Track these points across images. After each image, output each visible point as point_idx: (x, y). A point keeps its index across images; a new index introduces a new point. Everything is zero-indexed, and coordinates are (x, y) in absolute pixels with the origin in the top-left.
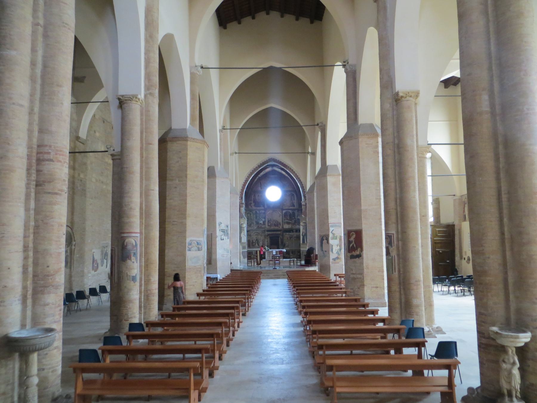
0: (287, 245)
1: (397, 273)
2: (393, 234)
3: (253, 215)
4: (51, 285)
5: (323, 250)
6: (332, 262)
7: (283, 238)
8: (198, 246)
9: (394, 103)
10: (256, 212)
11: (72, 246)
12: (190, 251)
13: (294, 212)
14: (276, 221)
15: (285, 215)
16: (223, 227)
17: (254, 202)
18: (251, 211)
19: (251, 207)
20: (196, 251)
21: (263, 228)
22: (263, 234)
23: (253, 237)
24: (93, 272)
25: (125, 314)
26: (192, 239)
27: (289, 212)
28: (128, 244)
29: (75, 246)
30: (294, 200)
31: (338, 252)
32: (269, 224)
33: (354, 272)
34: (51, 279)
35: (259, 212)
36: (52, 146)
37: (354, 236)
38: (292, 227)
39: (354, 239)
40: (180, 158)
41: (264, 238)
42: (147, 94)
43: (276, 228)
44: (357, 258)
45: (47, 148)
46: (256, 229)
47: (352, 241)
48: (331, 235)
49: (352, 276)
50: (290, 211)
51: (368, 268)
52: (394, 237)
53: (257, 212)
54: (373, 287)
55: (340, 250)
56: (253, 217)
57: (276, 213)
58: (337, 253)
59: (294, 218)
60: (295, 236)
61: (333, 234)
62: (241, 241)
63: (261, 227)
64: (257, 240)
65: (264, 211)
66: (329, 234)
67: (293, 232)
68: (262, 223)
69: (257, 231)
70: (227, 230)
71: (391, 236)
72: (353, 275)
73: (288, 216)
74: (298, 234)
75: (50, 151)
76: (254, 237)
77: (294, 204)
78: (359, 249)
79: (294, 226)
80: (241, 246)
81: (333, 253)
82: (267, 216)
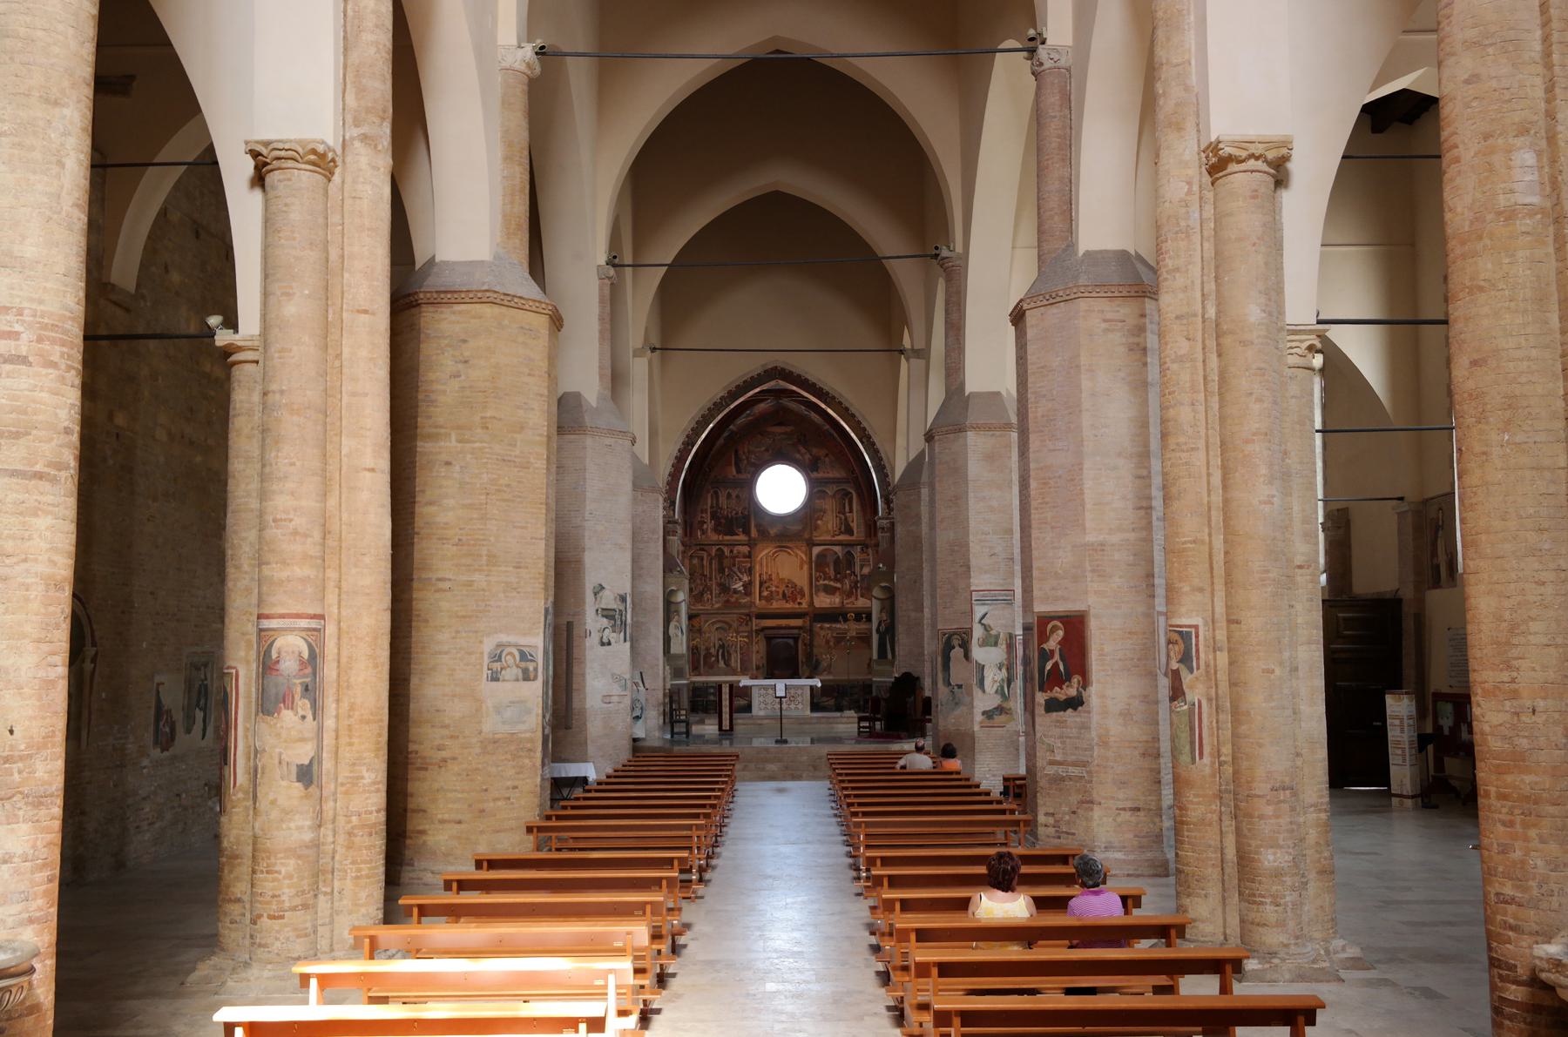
0: (824, 664)
1: (1207, 760)
2: (1196, 627)
3: (711, 564)
4: (21, 793)
5: (950, 684)
6: (981, 723)
7: (811, 640)
8: (523, 665)
9: (1207, 179)
10: (720, 554)
11: (83, 662)
12: (497, 680)
15: (821, 562)
16: (609, 600)
17: (712, 518)
18: (702, 547)
19: (704, 532)
20: (517, 680)
21: (744, 606)
22: (743, 628)
23: (709, 638)
24: (159, 750)
25: (273, 896)
26: (504, 638)
28: (283, 654)
29: (94, 660)
30: (851, 511)
31: (1002, 688)
32: (765, 593)
33: (1058, 758)
34: (20, 772)
35: (731, 551)
36: (26, 312)
37: (1061, 633)
39: (1060, 643)
40: (466, 362)
42: (352, 139)
43: (789, 606)
44: (1070, 710)
45: (8, 318)
46: (719, 609)
47: (1052, 652)
48: (978, 632)
49: (1050, 770)
50: (837, 549)
51: (1105, 744)
52: (1197, 637)
54: (1124, 809)
55: (1009, 681)
56: (711, 568)
58: (996, 692)
60: (854, 634)
61: (987, 628)
62: (669, 652)
63: (737, 605)
64: (722, 646)
65: (745, 549)
66: (971, 629)
67: (846, 620)
69: (720, 618)
70: (620, 611)
71: (1189, 634)
72: (1055, 768)
74: (863, 626)
75: (17, 328)
78: (1076, 679)
80: (667, 668)
81: (984, 691)
82: (757, 567)
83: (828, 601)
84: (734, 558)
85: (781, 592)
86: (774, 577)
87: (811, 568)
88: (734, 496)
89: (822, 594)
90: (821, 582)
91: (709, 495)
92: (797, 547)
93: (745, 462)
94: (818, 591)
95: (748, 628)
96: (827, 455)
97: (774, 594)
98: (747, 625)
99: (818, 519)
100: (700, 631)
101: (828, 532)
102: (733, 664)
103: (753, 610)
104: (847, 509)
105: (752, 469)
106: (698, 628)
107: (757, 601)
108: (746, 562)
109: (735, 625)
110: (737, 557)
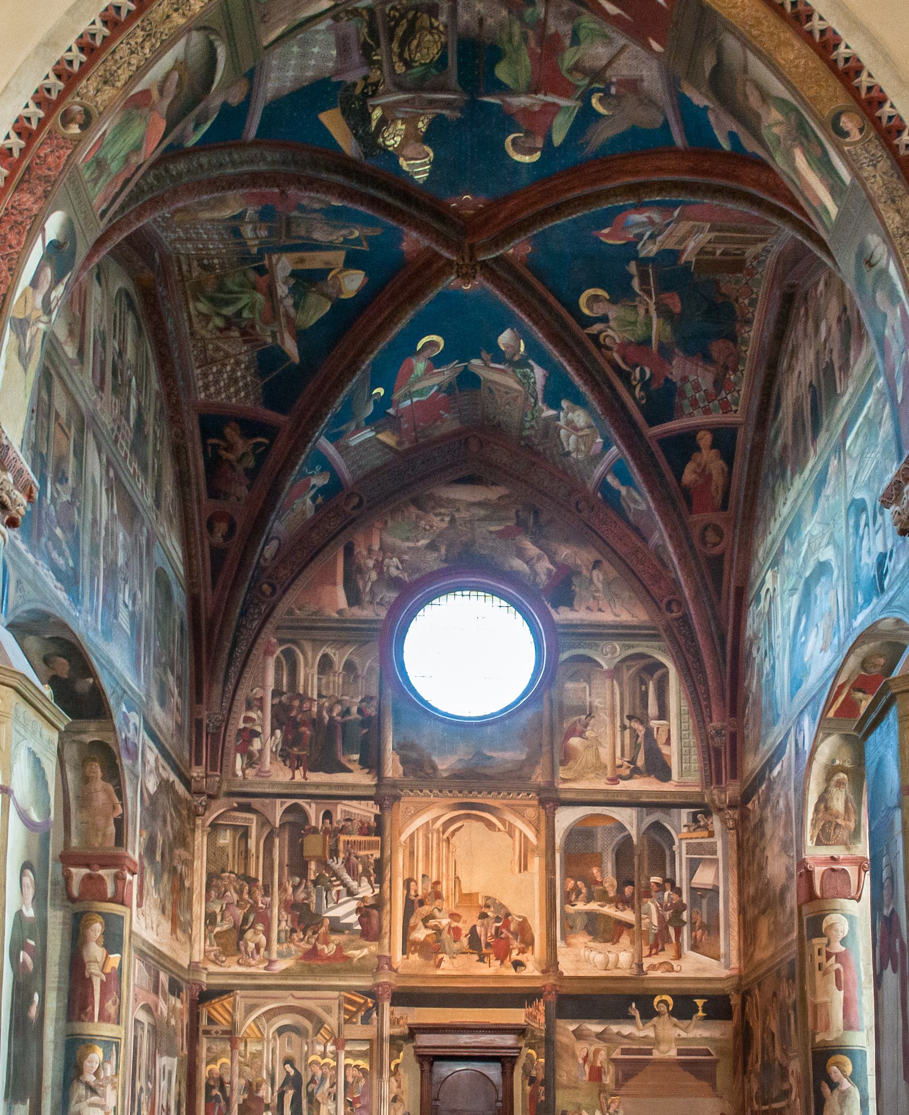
3: (268, 850)
7: (551, 1068)
13: (657, 826)
17: (277, 722)
19: (252, 760)
21: (360, 969)
22: (357, 1030)
23: (258, 1055)
27: (622, 828)
30: (663, 714)
32: (421, 934)
35: (328, 815)
38: (640, 966)
41: (363, 1064)
46: (286, 973)
50: (626, 816)
53: (306, 817)
57: (490, 825)
59: (661, 888)
60: (673, 1053)
64: (294, 1081)
65: (366, 811)
67: (648, 1013)
68: (354, 918)
73: (600, 865)
76: (267, 1057)
77: (665, 750)
79: (655, 960)
82: (400, 860)
83: (599, 958)
85: (465, 931)
86: (444, 889)
87: (550, 868)
88: (339, 666)
89: (581, 940)
90: (580, 906)
91: (271, 663)
92: (513, 809)
93: (374, 576)
94: (569, 928)
95: (370, 1032)
96: (596, 564)
97: (445, 936)
98: (366, 1020)
99: (572, 733)
100: (231, 1035)
101: (599, 767)
103: (384, 979)
104: (653, 708)
105: (392, 596)
106: (225, 1026)
107: (398, 957)
108: (370, 846)
109: (332, 1021)
110: (343, 830)
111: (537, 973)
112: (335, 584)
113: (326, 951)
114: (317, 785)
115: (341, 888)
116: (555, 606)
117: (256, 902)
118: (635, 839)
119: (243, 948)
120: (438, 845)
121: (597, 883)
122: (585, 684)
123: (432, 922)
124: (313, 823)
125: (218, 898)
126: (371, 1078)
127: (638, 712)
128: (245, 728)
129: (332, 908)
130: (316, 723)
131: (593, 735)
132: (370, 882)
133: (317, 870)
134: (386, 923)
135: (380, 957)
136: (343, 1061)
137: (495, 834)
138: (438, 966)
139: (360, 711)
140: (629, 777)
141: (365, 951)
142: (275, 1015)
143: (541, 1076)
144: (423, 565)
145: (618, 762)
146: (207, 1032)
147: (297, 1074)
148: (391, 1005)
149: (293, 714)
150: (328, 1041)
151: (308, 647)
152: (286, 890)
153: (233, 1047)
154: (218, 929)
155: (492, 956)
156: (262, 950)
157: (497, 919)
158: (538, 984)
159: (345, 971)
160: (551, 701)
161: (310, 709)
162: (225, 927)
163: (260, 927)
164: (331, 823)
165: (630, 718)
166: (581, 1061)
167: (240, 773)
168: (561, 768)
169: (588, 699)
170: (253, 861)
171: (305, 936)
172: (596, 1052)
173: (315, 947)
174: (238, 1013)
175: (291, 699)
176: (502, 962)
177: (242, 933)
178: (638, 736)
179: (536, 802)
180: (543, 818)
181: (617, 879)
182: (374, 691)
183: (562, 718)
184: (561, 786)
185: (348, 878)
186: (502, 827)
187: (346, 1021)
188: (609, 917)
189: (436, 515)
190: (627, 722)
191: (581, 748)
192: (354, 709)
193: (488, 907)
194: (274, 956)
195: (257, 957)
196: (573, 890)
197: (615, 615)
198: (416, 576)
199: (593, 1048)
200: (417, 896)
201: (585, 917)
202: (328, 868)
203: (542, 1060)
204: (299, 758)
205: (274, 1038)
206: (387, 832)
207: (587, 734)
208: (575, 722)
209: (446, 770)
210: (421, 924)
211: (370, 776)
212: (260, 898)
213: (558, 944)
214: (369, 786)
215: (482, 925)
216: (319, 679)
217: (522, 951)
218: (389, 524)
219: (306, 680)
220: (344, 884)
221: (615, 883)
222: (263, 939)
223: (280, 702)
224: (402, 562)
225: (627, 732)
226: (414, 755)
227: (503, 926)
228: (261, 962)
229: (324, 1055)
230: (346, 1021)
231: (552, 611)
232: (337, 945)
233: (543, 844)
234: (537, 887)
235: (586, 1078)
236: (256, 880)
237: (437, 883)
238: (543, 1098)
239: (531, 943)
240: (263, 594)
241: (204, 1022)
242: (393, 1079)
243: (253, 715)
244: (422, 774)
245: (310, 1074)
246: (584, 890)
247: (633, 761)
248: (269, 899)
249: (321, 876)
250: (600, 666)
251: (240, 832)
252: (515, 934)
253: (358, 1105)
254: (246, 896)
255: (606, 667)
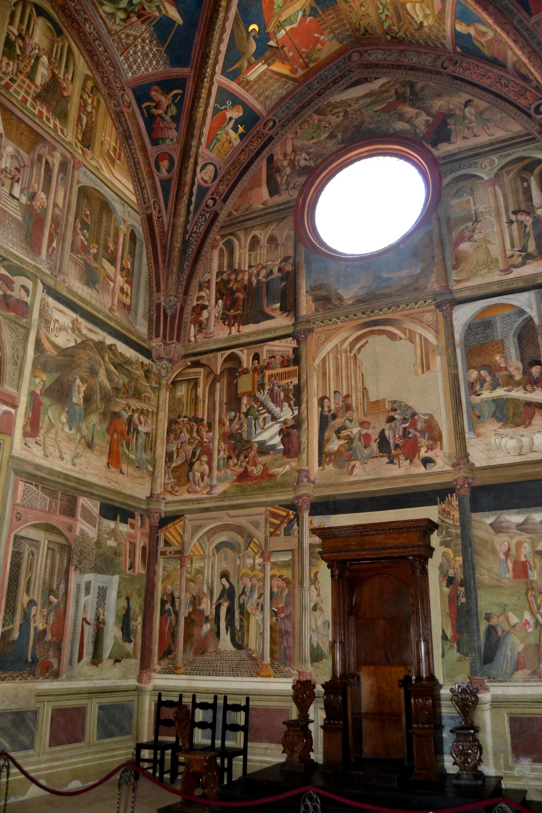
14: (396, 406)
17: (220, 295)
19: (201, 327)
23: (200, 572)
27: (521, 312)
32: (334, 445)
35: (256, 357)
41: (287, 573)
46: (224, 495)
57: (393, 337)
68: (277, 440)
69: (224, 518)
76: (207, 572)
84: (260, 371)
85: (375, 436)
86: (354, 401)
87: (452, 364)
90: (486, 394)
91: (216, 253)
92: (412, 318)
93: (288, 170)
95: (292, 542)
96: (467, 103)
97: (357, 444)
98: (288, 532)
99: (461, 239)
100: (180, 555)
102: (253, 643)
105: (303, 179)
106: (177, 547)
108: (289, 375)
109: (260, 535)
110: (268, 367)
111: (448, 468)
112: (260, 185)
113: (255, 472)
114: (248, 335)
115: (267, 414)
116: (435, 144)
117: (202, 438)
118: (536, 320)
119: (191, 478)
120: (347, 363)
121: (501, 369)
122: (467, 197)
123: (344, 433)
124: (245, 365)
125: (175, 439)
126: (294, 587)
127: (523, 207)
128: (198, 305)
129: (260, 434)
130: (247, 288)
131: (482, 236)
132: (290, 406)
133: (248, 403)
134: (303, 439)
135: (299, 471)
136: (269, 573)
137: (398, 342)
138: (351, 473)
139: (280, 270)
140: (523, 264)
141: (287, 468)
142: (214, 534)
143: (460, 576)
144: (324, 151)
145: (509, 253)
146: (163, 553)
147: (232, 587)
148: (310, 514)
149: (231, 285)
150: (256, 554)
151: (241, 234)
152: (224, 424)
153: (182, 566)
154: (174, 465)
155: (401, 457)
156: (206, 478)
157: (405, 420)
158: (448, 479)
159: (272, 487)
160: (439, 219)
161: (243, 279)
162: (180, 462)
163: (205, 458)
164: (259, 363)
165: (515, 213)
166: (502, 557)
167: (193, 339)
168: (454, 272)
169: (473, 208)
170: (200, 404)
171: (238, 460)
172: (519, 545)
173: (246, 469)
174: (186, 535)
175: (229, 275)
176: (411, 461)
177: (192, 464)
178: (526, 226)
179: (433, 307)
180: (441, 319)
181: (522, 361)
182: (291, 253)
183: (450, 229)
184: (455, 288)
185: (271, 405)
186: (402, 336)
187: (271, 534)
188: (518, 400)
189: (333, 115)
190: (513, 217)
191: (471, 250)
192: (276, 270)
193: (395, 410)
194: (215, 482)
195: (202, 484)
196: (477, 380)
197: (490, 135)
198: (319, 161)
199: (514, 541)
200: (330, 411)
201: (493, 406)
202: (257, 400)
203: (460, 559)
204: (235, 317)
205: (213, 554)
206: (303, 360)
207: (476, 237)
208: (463, 230)
209: (351, 298)
210: (334, 436)
211: (289, 318)
212: (204, 434)
213: (467, 436)
214: (287, 327)
215: (391, 428)
216: (250, 255)
217: (430, 448)
218: (299, 132)
219: (240, 259)
220: (269, 412)
221: (521, 366)
222: (206, 468)
223: (222, 279)
224: (308, 154)
225: (515, 226)
226: (324, 293)
227: (410, 426)
228: (205, 488)
229: (253, 568)
230: (271, 534)
231: (433, 150)
232: (264, 465)
233: (443, 343)
234: (440, 384)
235: (510, 575)
236: (203, 420)
237: (348, 396)
238: (463, 600)
239: (440, 439)
240: (207, 206)
241: (161, 544)
242: (313, 587)
243: (203, 294)
244: (331, 306)
245: (242, 586)
246: (488, 379)
247: (524, 249)
248: (211, 434)
249: (251, 407)
250: (481, 178)
251: (192, 384)
252: (422, 432)
253: (283, 615)
254: (195, 434)
255: (486, 178)
